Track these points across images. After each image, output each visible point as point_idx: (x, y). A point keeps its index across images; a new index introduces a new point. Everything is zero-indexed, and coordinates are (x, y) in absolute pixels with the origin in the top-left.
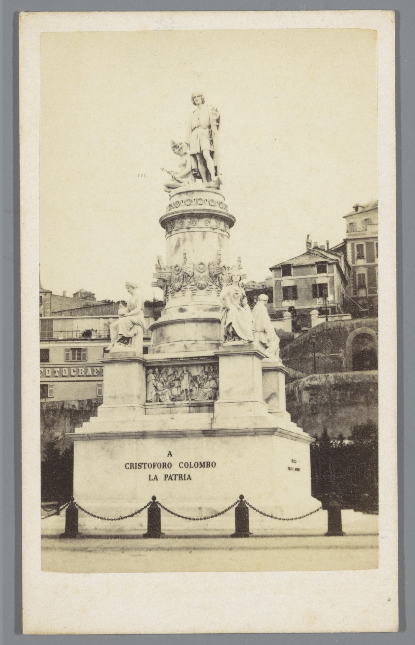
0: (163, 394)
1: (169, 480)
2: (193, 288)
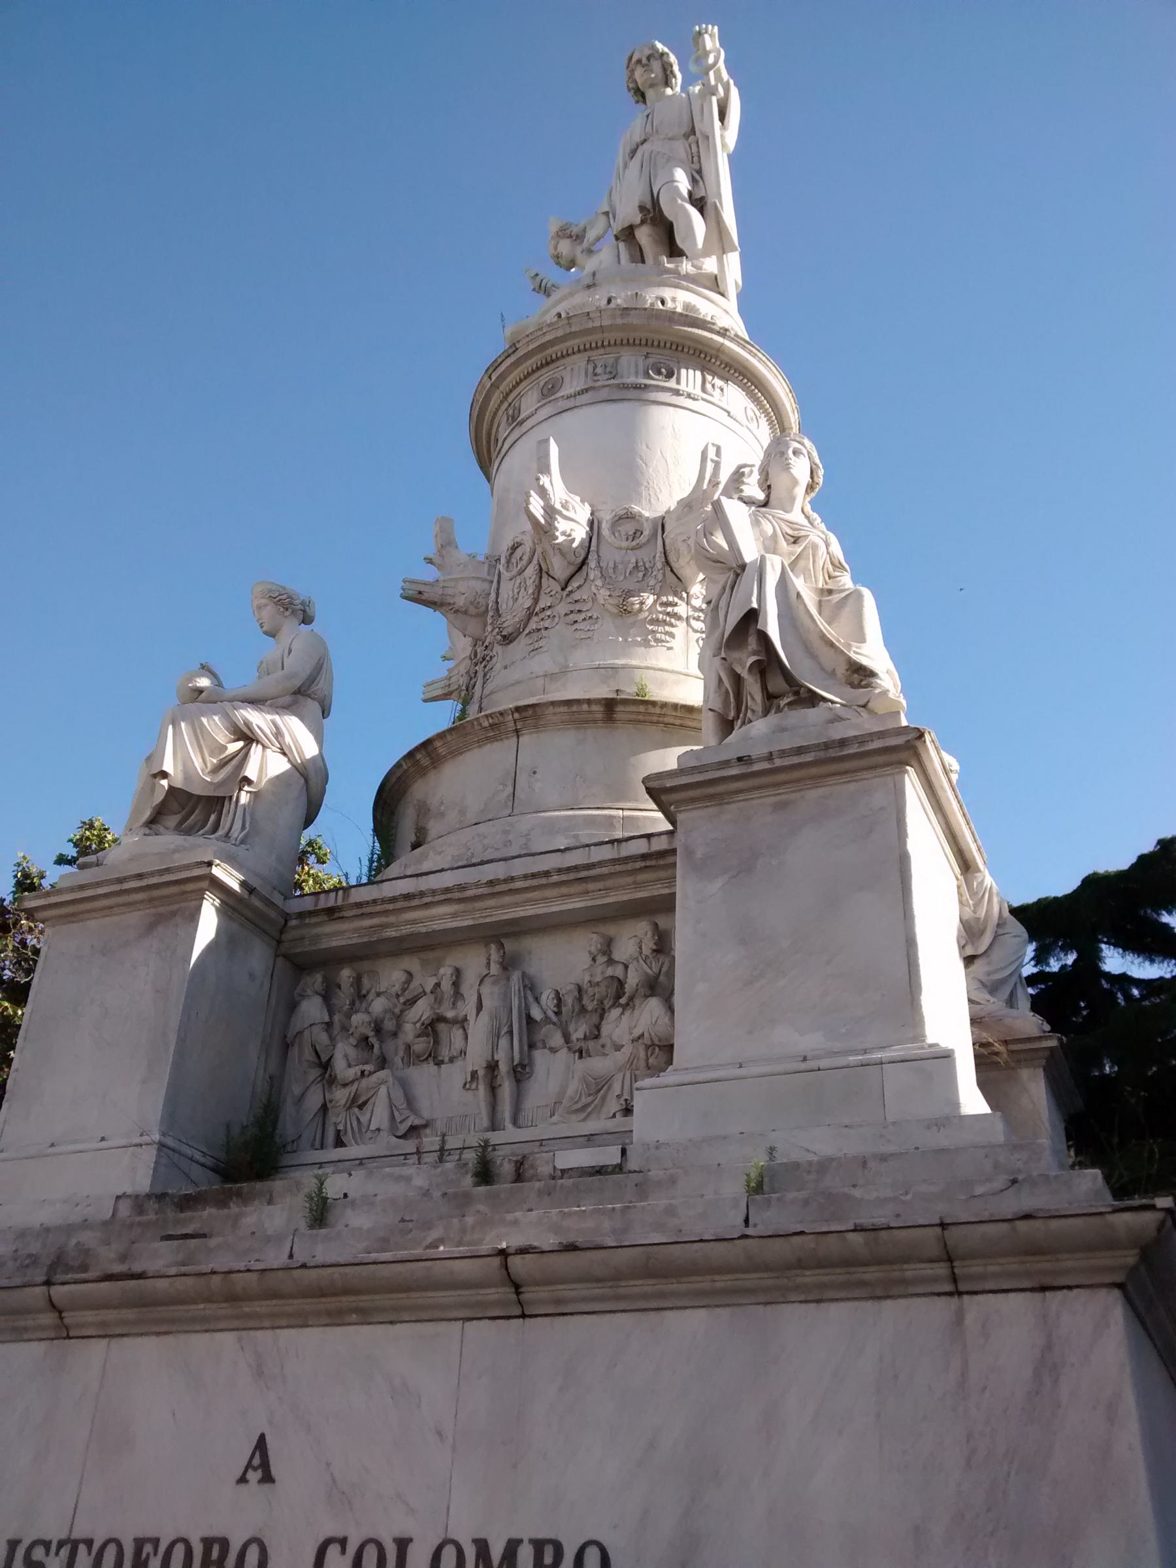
0: (360, 1102)
2: (579, 611)
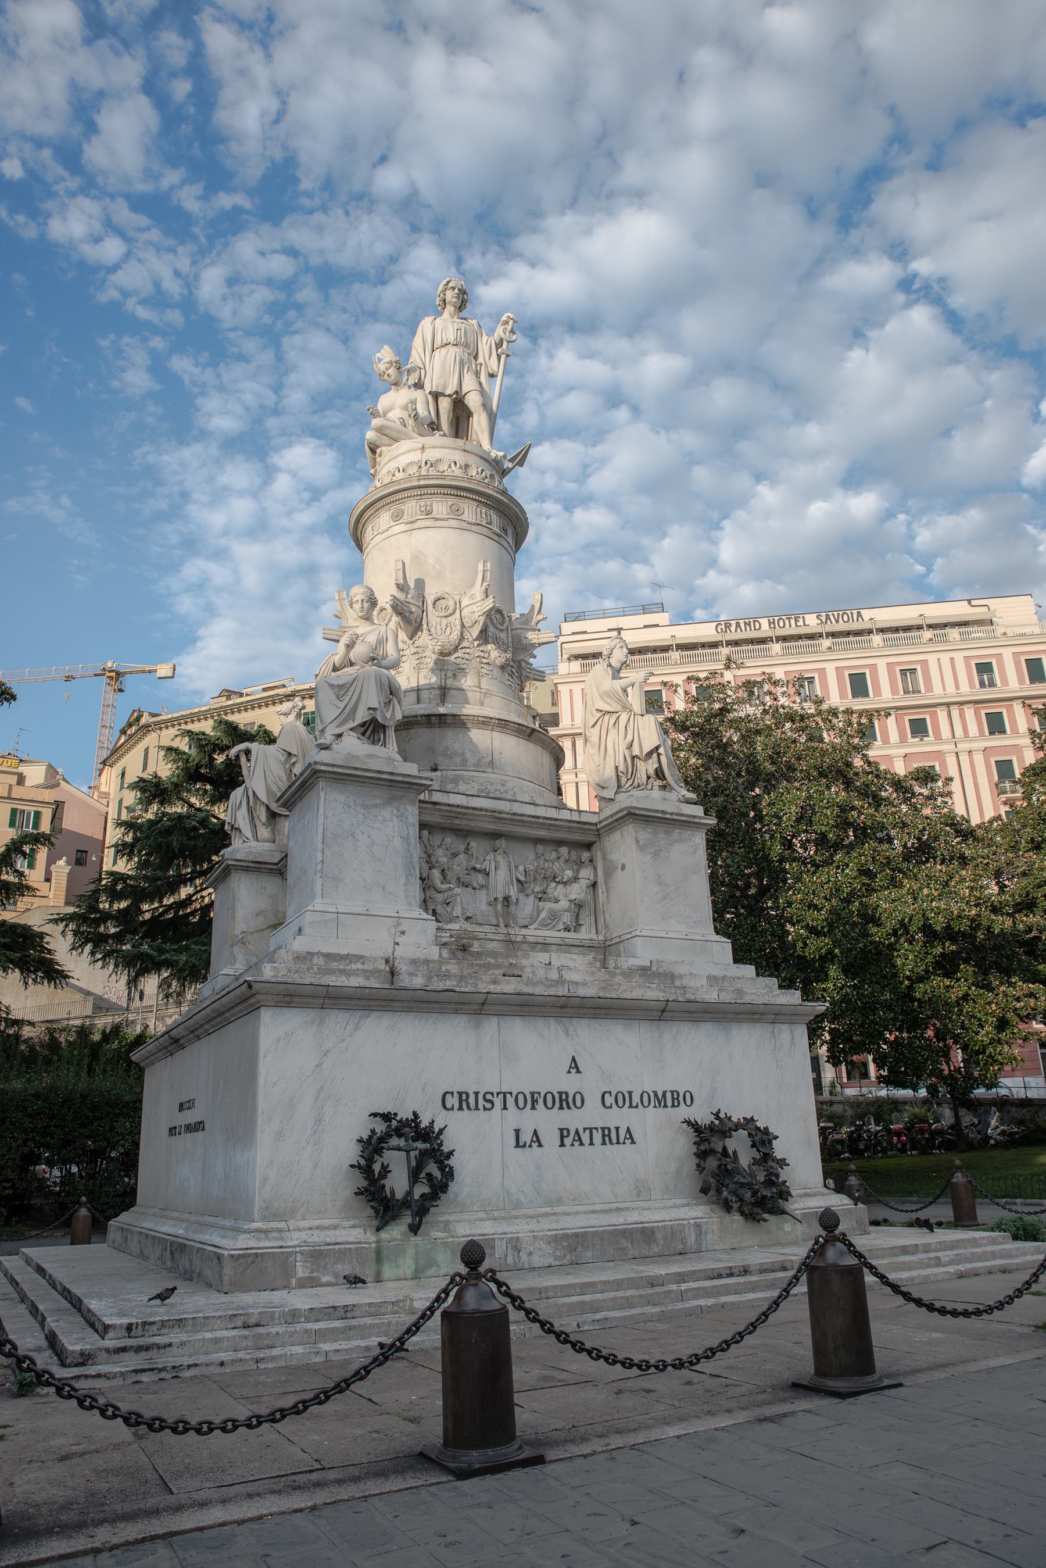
1: (572, 1145)
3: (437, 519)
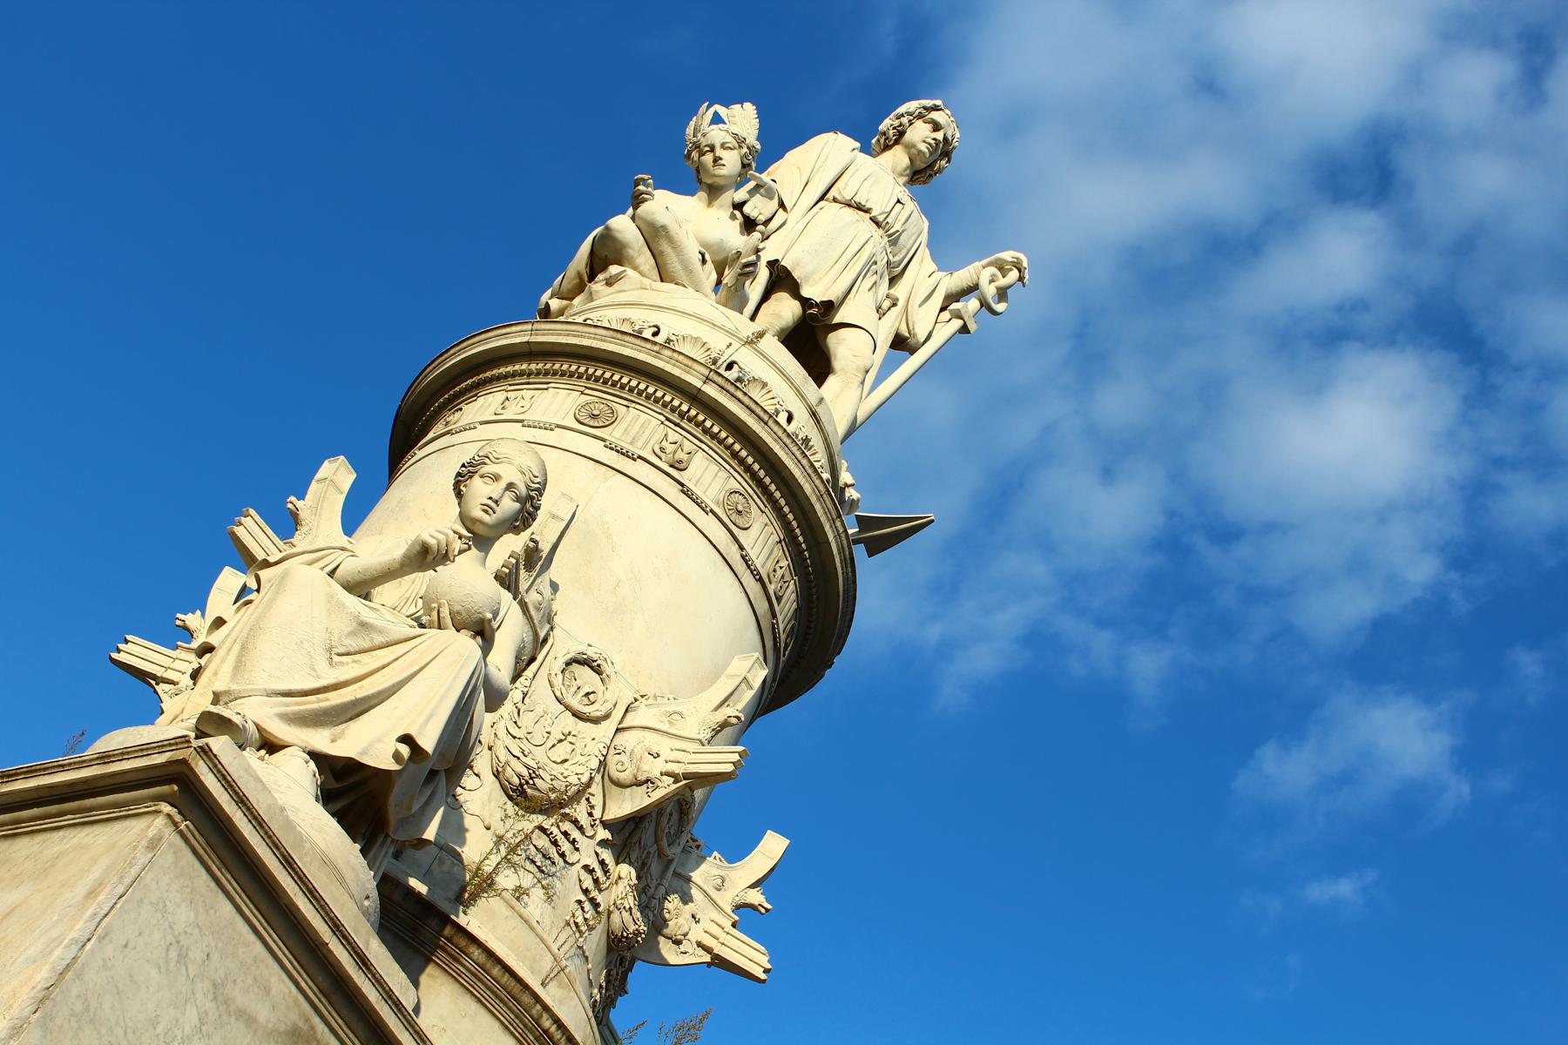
3: (686, 491)
